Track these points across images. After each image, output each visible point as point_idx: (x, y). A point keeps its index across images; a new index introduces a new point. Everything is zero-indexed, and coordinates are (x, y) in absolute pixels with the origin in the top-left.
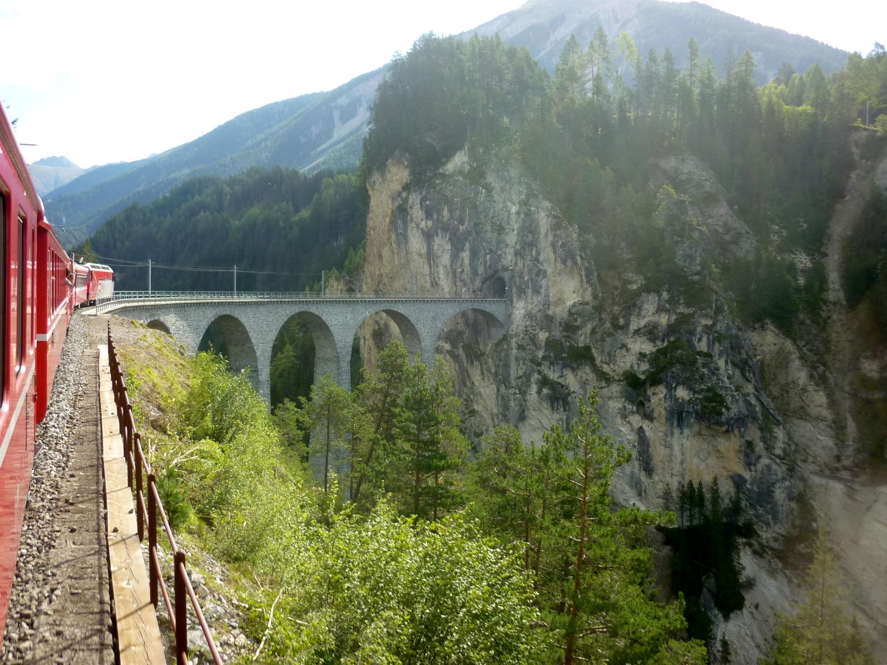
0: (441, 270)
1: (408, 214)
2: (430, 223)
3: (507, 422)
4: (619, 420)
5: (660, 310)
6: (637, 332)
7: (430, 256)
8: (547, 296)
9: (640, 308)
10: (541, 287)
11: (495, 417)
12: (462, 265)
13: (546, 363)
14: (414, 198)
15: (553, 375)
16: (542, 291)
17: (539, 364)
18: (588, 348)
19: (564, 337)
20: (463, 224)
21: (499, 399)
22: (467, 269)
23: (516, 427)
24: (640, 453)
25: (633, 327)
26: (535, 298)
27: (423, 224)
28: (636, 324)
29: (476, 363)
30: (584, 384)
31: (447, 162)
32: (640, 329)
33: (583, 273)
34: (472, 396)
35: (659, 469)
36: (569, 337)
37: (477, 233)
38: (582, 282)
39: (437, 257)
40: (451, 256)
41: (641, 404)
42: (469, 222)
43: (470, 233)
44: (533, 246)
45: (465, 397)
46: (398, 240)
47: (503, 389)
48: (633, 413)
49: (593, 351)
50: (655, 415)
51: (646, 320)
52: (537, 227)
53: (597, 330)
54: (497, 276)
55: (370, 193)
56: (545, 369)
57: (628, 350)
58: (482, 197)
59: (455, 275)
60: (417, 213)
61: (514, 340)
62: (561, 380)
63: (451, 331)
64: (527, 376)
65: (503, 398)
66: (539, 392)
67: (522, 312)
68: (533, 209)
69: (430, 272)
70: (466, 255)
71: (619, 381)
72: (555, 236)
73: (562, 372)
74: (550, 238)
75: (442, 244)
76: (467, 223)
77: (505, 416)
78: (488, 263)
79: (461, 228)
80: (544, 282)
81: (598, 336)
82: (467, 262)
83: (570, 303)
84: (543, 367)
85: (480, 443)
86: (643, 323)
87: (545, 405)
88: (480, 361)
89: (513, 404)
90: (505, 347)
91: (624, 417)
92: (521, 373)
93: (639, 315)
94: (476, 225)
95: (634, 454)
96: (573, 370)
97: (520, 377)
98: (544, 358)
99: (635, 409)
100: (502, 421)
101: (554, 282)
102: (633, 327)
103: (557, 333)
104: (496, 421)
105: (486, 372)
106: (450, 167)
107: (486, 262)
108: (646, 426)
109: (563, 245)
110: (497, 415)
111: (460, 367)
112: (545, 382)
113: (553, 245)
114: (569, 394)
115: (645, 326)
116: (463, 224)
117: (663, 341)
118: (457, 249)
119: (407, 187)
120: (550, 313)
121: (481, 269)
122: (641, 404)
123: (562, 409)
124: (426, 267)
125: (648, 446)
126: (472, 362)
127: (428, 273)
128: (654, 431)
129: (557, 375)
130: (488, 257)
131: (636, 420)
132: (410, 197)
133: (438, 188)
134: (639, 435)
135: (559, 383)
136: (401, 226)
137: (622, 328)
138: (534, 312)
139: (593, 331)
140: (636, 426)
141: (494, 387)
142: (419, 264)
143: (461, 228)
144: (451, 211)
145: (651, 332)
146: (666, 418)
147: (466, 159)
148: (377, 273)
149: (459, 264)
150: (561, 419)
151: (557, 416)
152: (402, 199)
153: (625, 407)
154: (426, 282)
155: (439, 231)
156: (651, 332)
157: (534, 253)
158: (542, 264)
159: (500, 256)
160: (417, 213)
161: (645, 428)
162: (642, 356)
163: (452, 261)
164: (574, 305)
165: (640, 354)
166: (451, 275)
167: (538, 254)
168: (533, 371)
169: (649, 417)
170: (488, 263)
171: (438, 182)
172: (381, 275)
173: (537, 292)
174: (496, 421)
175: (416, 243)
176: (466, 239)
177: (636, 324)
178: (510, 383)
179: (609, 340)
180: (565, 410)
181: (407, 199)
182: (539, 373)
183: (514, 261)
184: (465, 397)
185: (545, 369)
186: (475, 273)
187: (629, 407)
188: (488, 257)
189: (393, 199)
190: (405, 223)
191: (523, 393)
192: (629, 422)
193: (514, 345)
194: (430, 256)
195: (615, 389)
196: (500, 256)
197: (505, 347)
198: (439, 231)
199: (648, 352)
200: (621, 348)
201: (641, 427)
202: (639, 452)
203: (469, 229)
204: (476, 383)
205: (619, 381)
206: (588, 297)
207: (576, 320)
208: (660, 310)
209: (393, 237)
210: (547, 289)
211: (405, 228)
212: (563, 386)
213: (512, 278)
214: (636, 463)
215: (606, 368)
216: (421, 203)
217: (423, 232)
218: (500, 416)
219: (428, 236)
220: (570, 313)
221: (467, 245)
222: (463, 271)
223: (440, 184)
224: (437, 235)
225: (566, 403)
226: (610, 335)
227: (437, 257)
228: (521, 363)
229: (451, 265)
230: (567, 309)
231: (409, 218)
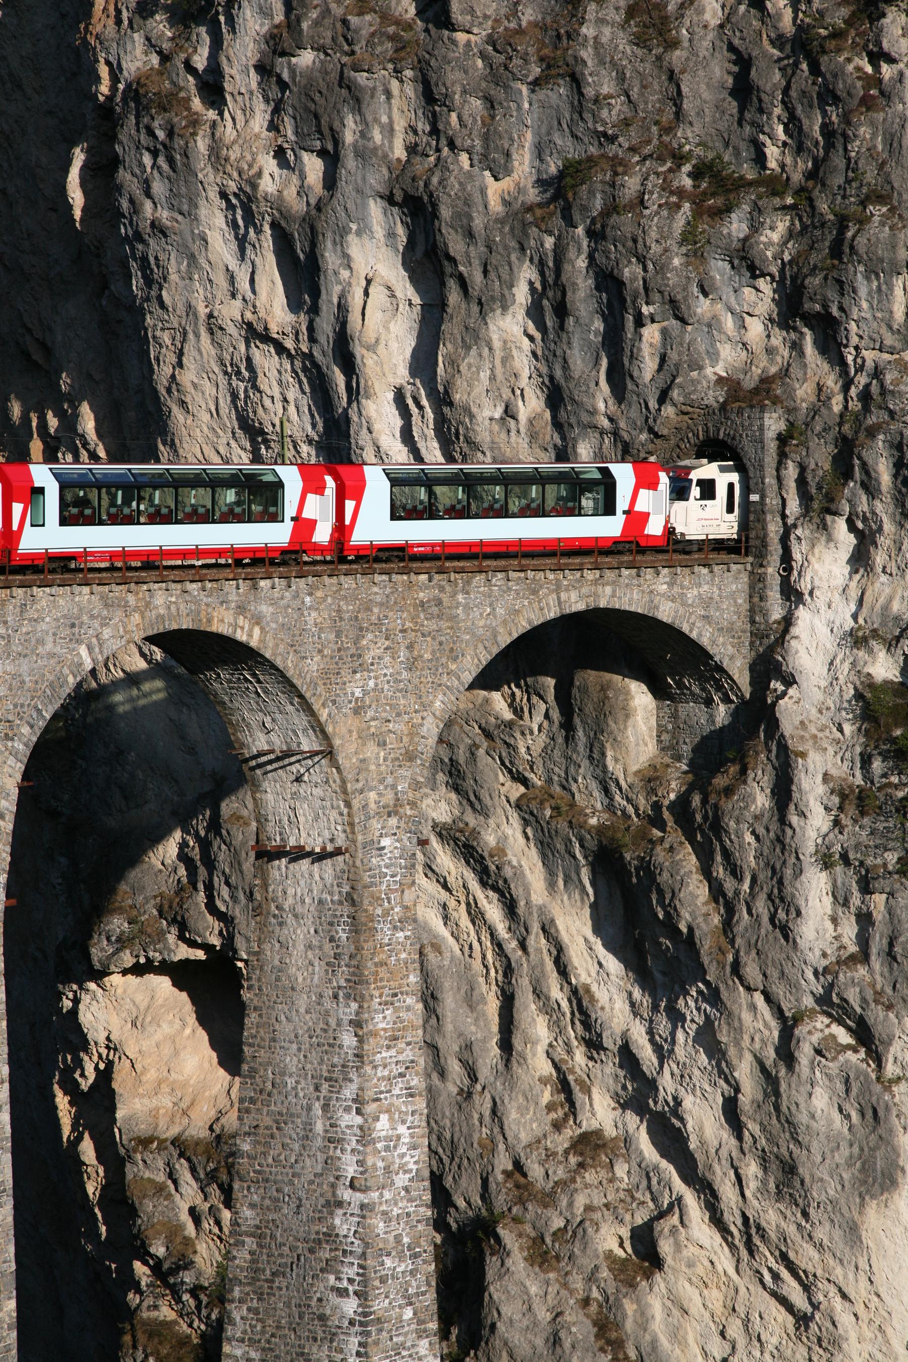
22: (532, 405)
42: (539, 152)
90: (762, 800)
111: (510, 907)
143: (495, 191)
218: (752, 1169)
222: (509, 413)
231: (202, 144)
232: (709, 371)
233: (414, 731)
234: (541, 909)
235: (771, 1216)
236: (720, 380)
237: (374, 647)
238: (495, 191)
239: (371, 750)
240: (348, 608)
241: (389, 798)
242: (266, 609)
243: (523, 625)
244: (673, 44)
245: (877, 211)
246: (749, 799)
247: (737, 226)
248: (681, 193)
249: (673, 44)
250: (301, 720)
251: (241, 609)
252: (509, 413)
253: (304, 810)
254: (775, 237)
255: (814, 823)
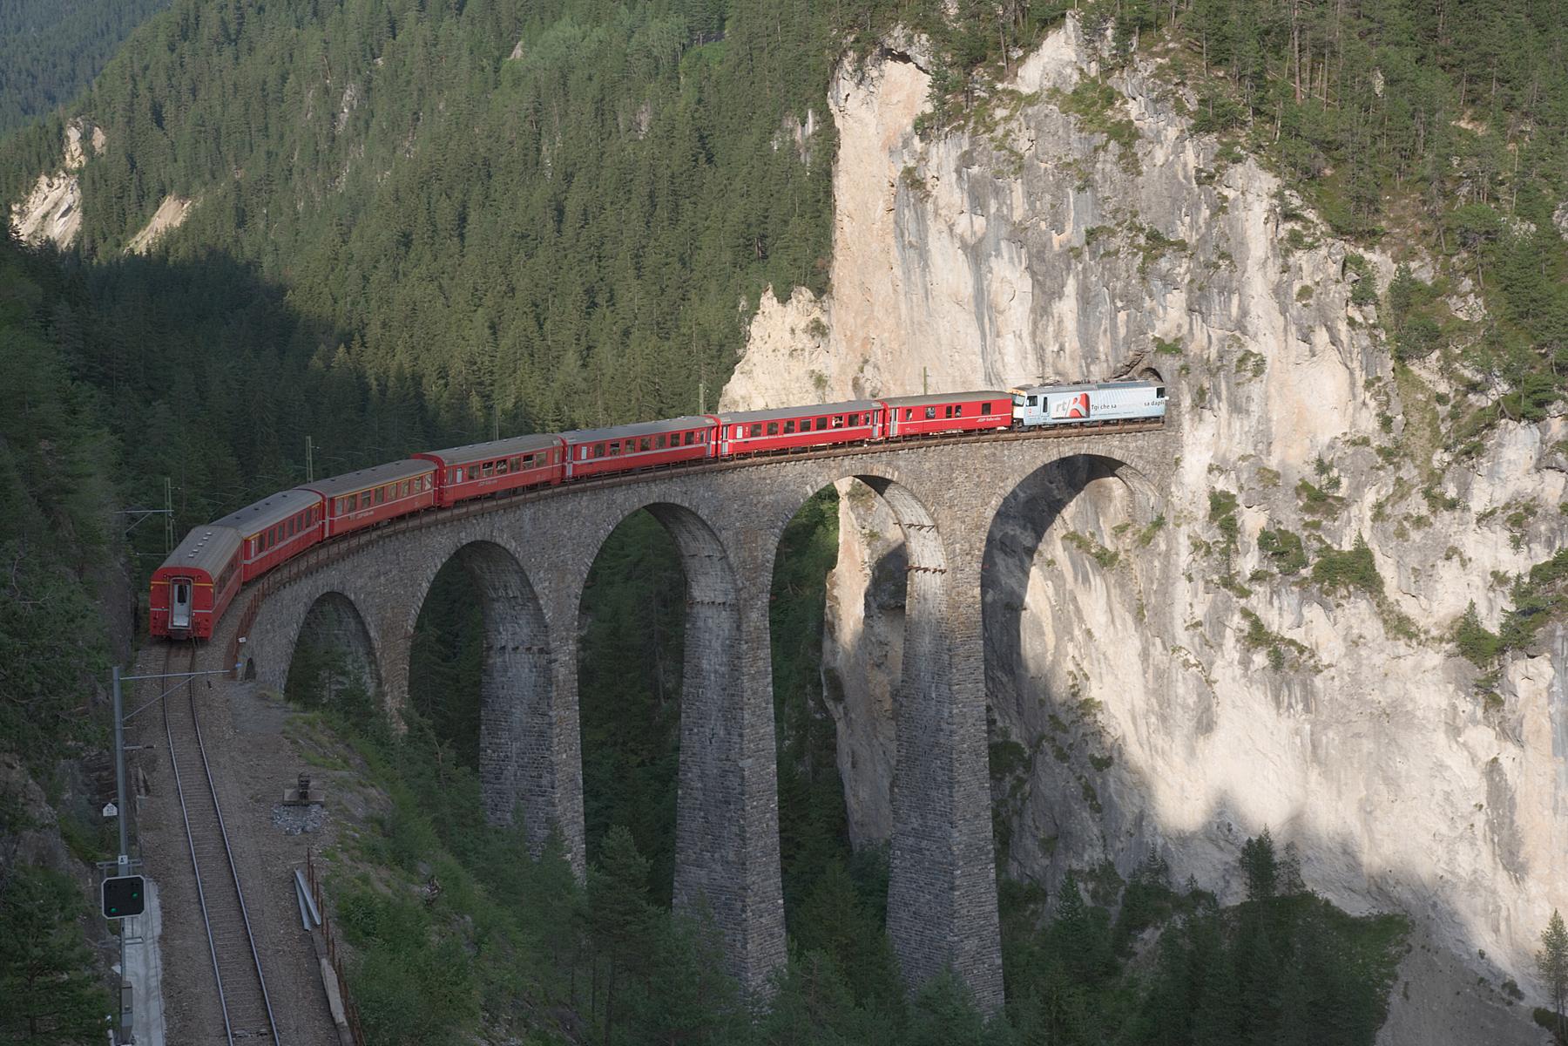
0: (1009, 345)
1: (928, 195)
2: (980, 222)
3: (1169, 734)
4: (1441, 738)
5: (1543, 464)
6: (1484, 518)
7: (983, 306)
8: (1265, 419)
9: (1496, 461)
10: (1249, 398)
11: (1141, 722)
12: (1058, 335)
13: (1260, 589)
14: (943, 155)
15: (1279, 617)
16: (1253, 407)
17: (1245, 594)
18: (1363, 554)
19: (1306, 525)
20: (1060, 231)
21: (1150, 675)
22: (1072, 343)
23: (1192, 752)
24: (1493, 827)
25: (1478, 504)
26: (1237, 424)
27: (962, 224)
28: (1482, 497)
29: (1096, 581)
30: (1355, 643)
31: (1022, 60)
32: (1492, 513)
33: (1355, 365)
34: (1085, 665)
35: (1539, 868)
36: (1316, 525)
37: (1093, 254)
38: (1353, 384)
39: (1001, 313)
40: (1033, 310)
41: (1495, 702)
42: (1077, 224)
43: (1077, 253)
44: (1231, 292)
45: (1071, 666)
46: (904, 259)
47: (1157, 650)
48: (1475, 722)
49: (1379, 558)
50: (1527, 727)
51: (1511, 488)
52: (1242, 243)
53: (1388, 510)
54: (1141, 366)
55: (838, 123)
56: (1258, 601)
57: (1464, 563)
58: (1107, 164)
59: (1042, 360)
60: (948, 192)
61: (1184, 529)
62: (1297, 635)
63: (1031, 501)
64: (1217, 622)
65: (1161, 675)
66: (1245, 663)
67: (1207, 458)
68: (1230, 194)
69: (984, 348)
70: (1067, 307)
71: (1441, 639)
72: (1285, 269)
73: (1301, 615)
74: (1273, 273)
75: (1010, 278)
76: (1069, 228)
77: (1163, 719)
78: (1122, 332)
79: (1057, 240)
80: (1255, 389)
81: (1392, 527)
82: (1071, 324)
83: (1324, 439)
84: (1254, 600)
85: (1105, 784)
86: (1502, 496)
87: (1259, 695)
88: (1104, 577)
89: (1181, 690)
90: (1163, 547)
91: (1454, 730)
92: (1200, 613)
93: (1492, 474)
94: (1091, 234)
95: (1480, 820)
96: (1325, 607)
97: (1199, 624)
98: (1257, 577)
99: (1480, 713)
100: (1156, 731)
101: (1282, 385)
102: (1478, 504)
103: (1291, 519)
104: (1143, 730)
105: (1117, 607)
106: (1032, 74)
107: (1114, 326)
108: (1508, 755)
109: (1305, 292)
110: (1146, 716)
112: (1258, 635)
113: (1278, 291)
114: (1317, 670)
115: (1507, 506)
116: (1060, 231)
117: (1550, 544)
118: (1045, 295)
119: (924, 128)
120: (1273, 463)
121: (1103, 347)
122: (1495, 702)
123: (1300, 706)
124: (974, 331)
125: (1512, 805)
126: (1086, 580)
127: (978, 350)
128: (1532, 772)
129: (1289, 619)
130: (1122, 316)
131: (1483, 739)
132: (933, 150)
133: (1000, 132)
134: (1491, 780)
135: (1292, 642)
136: (912, 226)
137: (1452, 505)
138: (1233, 458)
139: (1379, 512)
140: (1485, 757)
141: (1134, 644)
142: (957, 325)
144: (1029, 195)
145: (1519, 518)
146: (1554, 741)
147: (1069, 53)
148: (861, 334)
149: (1051, 329)
150: (1297, 732)
151: (1286, 724)
152: (913, 154)
153: (1454, 707)
154: (974, 371)
155: (1003, 244)
156: (1519, 518)
157: (1234, 310)
158: (1254, 338)
159: (1152, 311)
160: (948, 192)
161: (1506, 764)
162: (1499, 578)
163: (1035, 323)
164: (1331, 447)
165: (1495, 574)
166: (1031, 358)
167: (1244, 313)
168: (1228, 609)
169: (1510, 732)
170: (1122, 332)
171: (1000, 113)
172: (867, 341)
173: (1237, 408)
174: (1143, 730)
175: (950, 270)
176: (1068, 269)
177: (1482, 497)
178: (1174, 639)
179: (1416, 536)
180: (1307, 709)
181: (923, 158)
182: (1246, 614)
183: (1186, 328)
184: (1071, 666)
185: (1258, 601)
186: (1090, 355)
187: (1466, 706)
188: (1122, 316)
189: (891, 152)
190: (921, 218)
191: (1206, 667)
192: (1465, 745)
193: (1184, 544)
194: (983, 306)
195: (1433, 658)
196: (1152, 311)
197: (1163, 547)
198: (1003, 244)
199: (1512, 574)
200: (1448, 558)
201: (1495, 760)
202: (1489, 822)
203: (1078, 242)
204: (1096, 634)
205: (1441, 639)
206: (1369, 424)
207: (1336, 483)
208: (1543, 464)
209: (895, 252)
210: (1267, 398)
211: (923, 233)
212: (1302, 650)
213: (1186, 369)
214: (1486, 850)
215: (1409, 607)
216: (958, 172)
217: (964, 246)
218: (1153, 719)
219: (976, 253)
220: (1322, 467)
221: (1071, 286)
222: (1062, 349)
223: (1007, 119)
224: (999, 254)
225: (1309, 695)
226: (1420, 522)
227: (1001, 313)
228: (1201, 584)
229: (1034, 334)
230: (1315, 455)
231: (930, 207)
232: (1150, 335)
233: (981, 515)
234: (1071, 592)
235: (1160, 740)
236: (1155, 339)
237: (959, 477)
238: (1057, 240)
239: (957, 525)
240: (946, 460)
241: (967, 546)
242: (901, 463)
243: (1039, 464)
244: (1139, 173)
245: (1223, 263)
246: (1157, 545)
247: (1164, 264)
248: (1139, 247)
249: (1139, 173)
250: (922, 512)
251: (889, 464)
252: (1062, 349)
253: (927, 553)
254: (1182, 271)
255: (1184, 558)
